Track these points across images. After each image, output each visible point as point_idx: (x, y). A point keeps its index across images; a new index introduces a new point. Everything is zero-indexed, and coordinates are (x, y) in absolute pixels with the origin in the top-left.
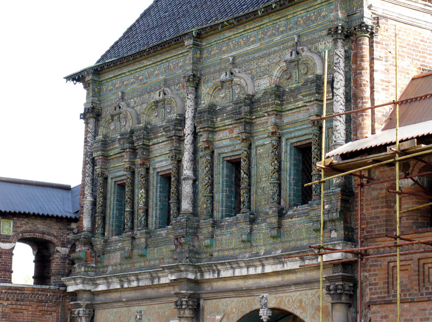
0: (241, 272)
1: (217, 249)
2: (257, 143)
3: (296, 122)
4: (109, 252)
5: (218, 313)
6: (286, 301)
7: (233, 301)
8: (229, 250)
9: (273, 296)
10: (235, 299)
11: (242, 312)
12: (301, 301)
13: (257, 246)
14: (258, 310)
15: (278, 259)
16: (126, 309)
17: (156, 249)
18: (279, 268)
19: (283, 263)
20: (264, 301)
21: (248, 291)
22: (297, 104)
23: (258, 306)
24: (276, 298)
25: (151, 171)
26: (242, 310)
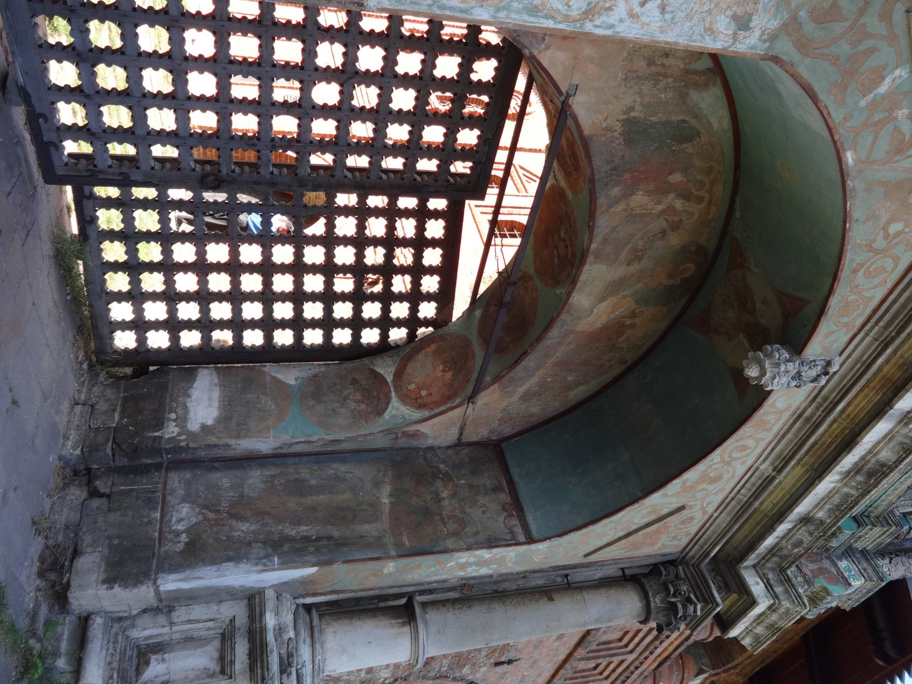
11: (855, 272)
23: (815, 348)
24: (781, 412)
26: (861, 274)
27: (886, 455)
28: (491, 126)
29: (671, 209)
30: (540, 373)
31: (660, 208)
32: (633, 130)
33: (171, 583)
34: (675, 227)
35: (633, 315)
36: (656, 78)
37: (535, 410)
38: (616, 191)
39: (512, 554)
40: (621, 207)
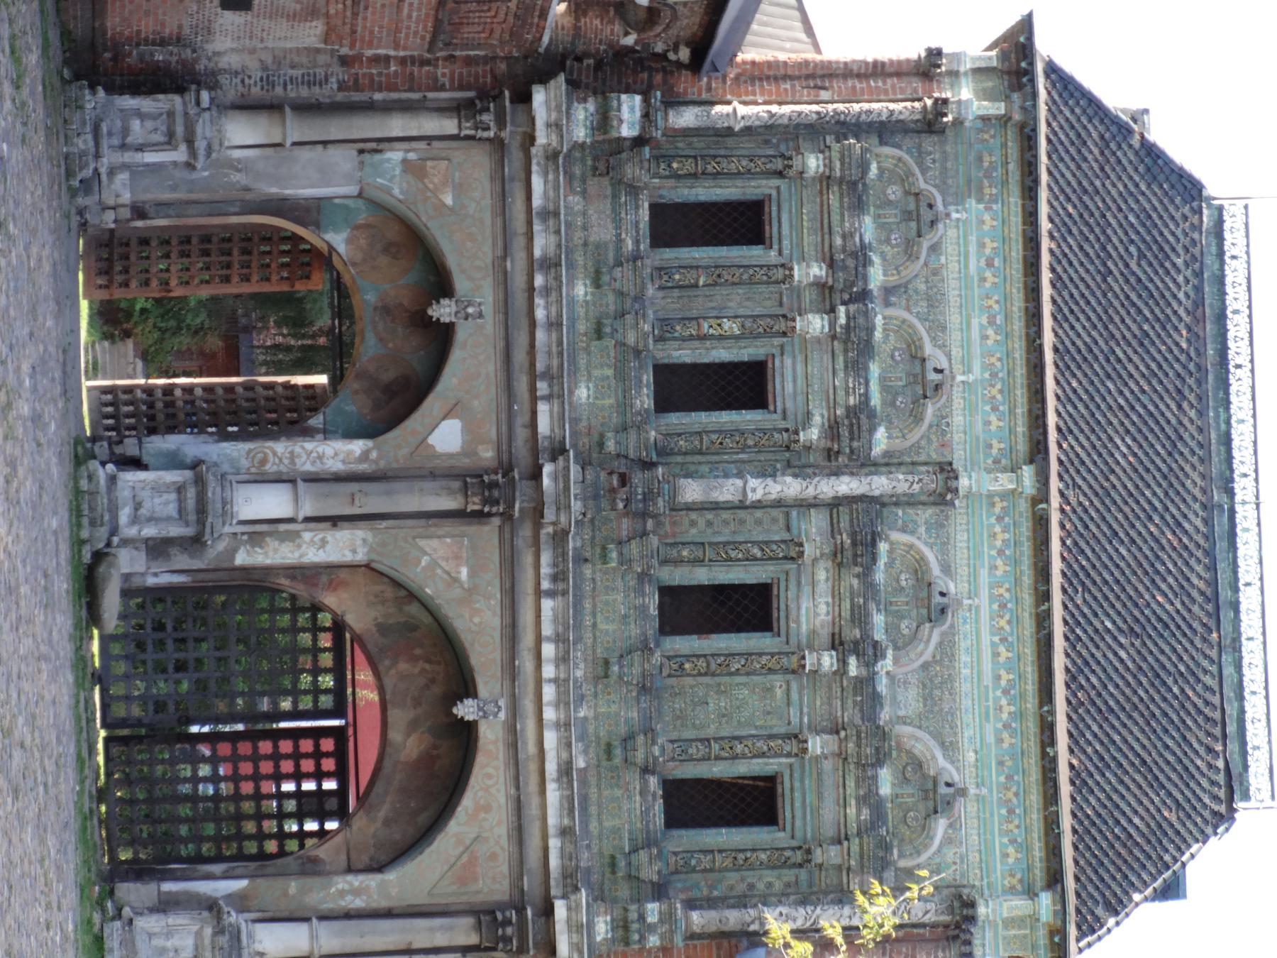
0: (549, 661)
1: (598, 576)
2: (794, 686)
3: (820, 797)
4: (615, 196)
5: (472, 574)
6: (490, 770)
7: (494, 614)
8: (594, 615)
9: (500, 734)
10: (497, 622)
12: (487, 808)
13: (596, 695)
14: (474, 695)
15: (566, 770)
16: (489, 260)
17: (610, 372)
18: (551, 767)
19: (558, 780)
20: (491, 708)
21: (511, 672)
22: (853, 802)
23: (483, 691)
24: (495, 742)
25: (777, 341)
27: (564, 755)
28: (339, 670)
29: (423, 671)
30: (389, 799)
31: (417, 671)
32: (383, 629)
33: (168, 886)
34: (433, 681)
35: (435, 747)
36: (383, 602)
37: (397, 836)
38: (387, 662)
39: (373, 884)
40: (393, 672)
